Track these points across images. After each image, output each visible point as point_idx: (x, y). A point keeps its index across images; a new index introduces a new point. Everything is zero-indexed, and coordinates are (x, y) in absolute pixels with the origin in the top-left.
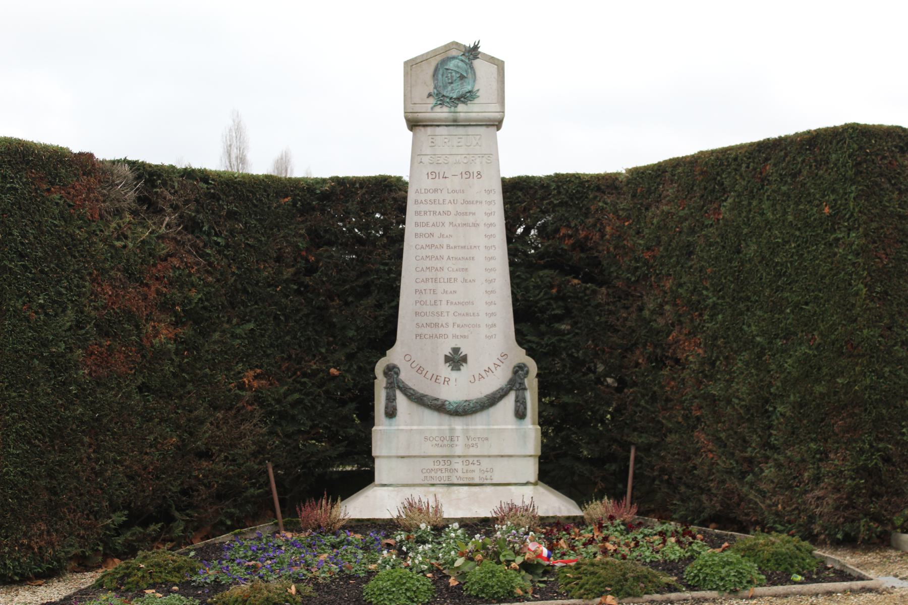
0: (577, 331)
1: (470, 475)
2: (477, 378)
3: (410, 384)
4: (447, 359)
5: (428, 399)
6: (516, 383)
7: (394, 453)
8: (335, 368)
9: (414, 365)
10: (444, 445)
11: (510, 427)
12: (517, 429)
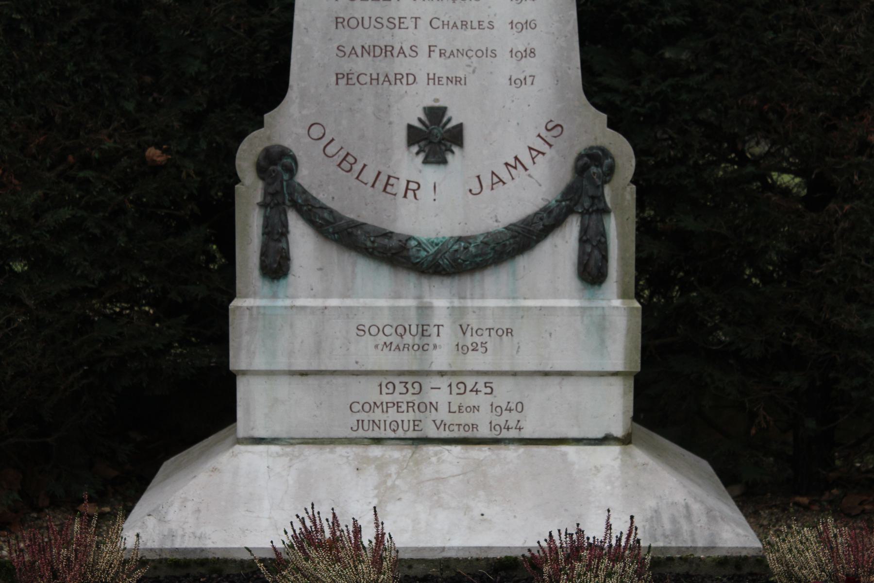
0: (718, 65)
1: (466, 418)
2: (487, 181)
3: (323, 197)
4: (414, 136)
5: (367, 234)
6: (582, 194)
7: (282, 364)
8: (158, 146)
9: (331, 150)
10: (406, 347)
11: (566, 303)
12: (583, 309)
